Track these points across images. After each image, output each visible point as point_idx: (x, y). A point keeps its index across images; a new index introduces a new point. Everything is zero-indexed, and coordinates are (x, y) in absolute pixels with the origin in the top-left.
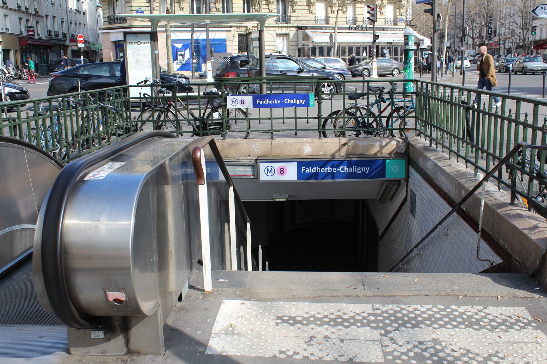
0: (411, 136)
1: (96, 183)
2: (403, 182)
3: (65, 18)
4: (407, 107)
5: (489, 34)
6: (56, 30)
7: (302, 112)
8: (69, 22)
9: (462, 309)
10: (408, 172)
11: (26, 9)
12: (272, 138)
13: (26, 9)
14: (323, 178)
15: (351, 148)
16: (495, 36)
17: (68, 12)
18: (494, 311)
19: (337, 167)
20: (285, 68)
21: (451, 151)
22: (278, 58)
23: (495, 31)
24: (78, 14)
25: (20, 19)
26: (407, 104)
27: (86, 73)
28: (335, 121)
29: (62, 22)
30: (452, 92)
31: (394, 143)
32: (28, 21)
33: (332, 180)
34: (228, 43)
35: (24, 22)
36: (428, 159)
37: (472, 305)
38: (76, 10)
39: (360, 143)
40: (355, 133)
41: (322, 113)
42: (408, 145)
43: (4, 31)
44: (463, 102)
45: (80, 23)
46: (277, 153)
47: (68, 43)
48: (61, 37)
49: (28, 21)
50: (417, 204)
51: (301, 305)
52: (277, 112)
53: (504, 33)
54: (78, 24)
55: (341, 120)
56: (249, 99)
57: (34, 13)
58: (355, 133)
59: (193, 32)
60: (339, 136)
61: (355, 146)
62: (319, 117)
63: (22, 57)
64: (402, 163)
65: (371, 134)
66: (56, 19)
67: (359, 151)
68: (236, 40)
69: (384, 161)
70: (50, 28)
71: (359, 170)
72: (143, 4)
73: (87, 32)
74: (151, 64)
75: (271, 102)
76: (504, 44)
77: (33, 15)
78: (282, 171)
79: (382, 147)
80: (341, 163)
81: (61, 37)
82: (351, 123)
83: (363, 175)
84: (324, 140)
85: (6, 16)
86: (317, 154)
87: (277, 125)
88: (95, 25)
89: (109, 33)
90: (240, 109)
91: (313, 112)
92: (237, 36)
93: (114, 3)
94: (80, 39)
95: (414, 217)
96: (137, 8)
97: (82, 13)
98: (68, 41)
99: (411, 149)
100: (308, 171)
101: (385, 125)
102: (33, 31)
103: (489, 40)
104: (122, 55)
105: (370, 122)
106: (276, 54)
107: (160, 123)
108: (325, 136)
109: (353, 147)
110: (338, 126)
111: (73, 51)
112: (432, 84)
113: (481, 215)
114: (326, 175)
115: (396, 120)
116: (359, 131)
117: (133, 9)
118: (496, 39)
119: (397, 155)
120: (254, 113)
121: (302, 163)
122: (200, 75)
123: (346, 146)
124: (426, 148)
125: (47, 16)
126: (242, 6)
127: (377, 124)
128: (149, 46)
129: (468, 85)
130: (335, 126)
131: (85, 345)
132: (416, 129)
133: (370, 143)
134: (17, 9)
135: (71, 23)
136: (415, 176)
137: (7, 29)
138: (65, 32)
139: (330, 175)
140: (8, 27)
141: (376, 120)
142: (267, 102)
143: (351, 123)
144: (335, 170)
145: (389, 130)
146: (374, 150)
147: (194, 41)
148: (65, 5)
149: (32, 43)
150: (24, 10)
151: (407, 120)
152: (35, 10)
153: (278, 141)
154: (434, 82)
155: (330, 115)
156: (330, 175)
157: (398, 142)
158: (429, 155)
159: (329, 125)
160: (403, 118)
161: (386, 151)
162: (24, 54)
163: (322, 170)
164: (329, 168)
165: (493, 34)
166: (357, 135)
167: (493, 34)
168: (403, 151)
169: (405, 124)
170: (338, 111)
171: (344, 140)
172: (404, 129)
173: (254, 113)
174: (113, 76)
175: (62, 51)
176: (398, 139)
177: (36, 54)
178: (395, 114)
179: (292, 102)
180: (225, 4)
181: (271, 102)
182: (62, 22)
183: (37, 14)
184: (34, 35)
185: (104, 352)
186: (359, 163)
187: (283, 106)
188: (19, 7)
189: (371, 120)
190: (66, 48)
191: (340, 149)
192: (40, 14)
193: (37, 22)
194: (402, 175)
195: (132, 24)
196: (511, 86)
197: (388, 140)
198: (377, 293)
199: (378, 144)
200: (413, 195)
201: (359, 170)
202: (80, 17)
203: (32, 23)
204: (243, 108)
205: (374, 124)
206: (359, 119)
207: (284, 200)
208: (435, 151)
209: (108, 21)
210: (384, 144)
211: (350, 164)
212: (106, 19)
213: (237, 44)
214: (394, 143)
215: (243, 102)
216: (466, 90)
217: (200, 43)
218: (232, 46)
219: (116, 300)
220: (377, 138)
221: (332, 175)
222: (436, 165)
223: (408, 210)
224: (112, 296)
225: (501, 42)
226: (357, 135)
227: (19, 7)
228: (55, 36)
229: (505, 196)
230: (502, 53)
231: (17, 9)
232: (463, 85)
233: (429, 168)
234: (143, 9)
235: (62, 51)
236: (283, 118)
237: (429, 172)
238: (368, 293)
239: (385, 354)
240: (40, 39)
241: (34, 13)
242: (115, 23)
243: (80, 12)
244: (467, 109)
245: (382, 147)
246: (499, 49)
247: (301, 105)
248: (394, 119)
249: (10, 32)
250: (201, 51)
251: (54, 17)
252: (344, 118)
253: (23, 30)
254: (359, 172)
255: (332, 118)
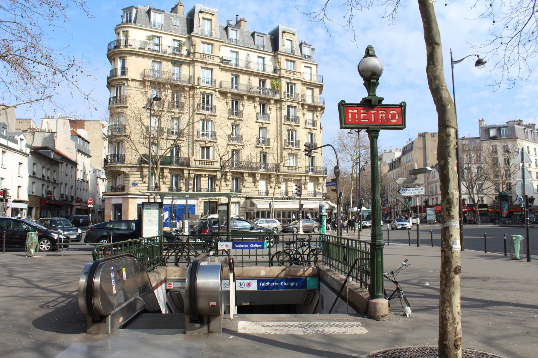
0: (320, 265)
1: (204, 267)
2: (317, 291)
3: (74, 185)
4: (318, 249)
5: (383, 202)
6: (67, 194)
7: (260, 251)
8: (76, 188)
9: (335, 323)
10: (319, 285)
11: (48, 178)
12: (243, 267)
13: (48, 178)
14: (272, 289)
15: (287, 272)
16: (388, 203)
17: (76, 181)
18: (347, 323)
19: (280, 283)
20: (242, 226)
21: (339, 270)
22: (237, 220)
23: (387, 200)
24: (83, 183)
25: (43, 185)
26: (318, 247)
27: (111, 226)
28: (278, 257)
29: (72, 188)
30: (352, 243)
31: (311, 269)
32: (48, 186)
33: (277, 290)
34: (196, 207)
35: (45, 187)
36: (328, 275)
37: (339, 321)
38: (82, 180)
39: (292, 269)
40: (289, 264)
41: (271, 252)
42: (319, 270)
43: (31, 193)
44: (342, 244)
45: (84, 189)
46: (245, 274)
47: (74, 203)
48: (70, 199)
49: (48, 186)
50: (324, 302)
51: (270, 322)
52: (246, 252)
53: (394, 201)
54: (82, 189)
55: (281, 256)
56: (230, 244)
57: (53, 181)
58: (289, 264)
59: (173, 199)
60: (281, 266)
61: (290, 271)
62: (269, 254)
63: (41, 213)
64: (316, 279)
65: (299, 265)
66: (68, 186)
67: (292, 273)
68: (202, 205)
69: (306, 279)
70: (62, 192)
71: (292, 284)
72: (137, 179)
73: (88, 195)
74: (158, 222)
75: (243, 246)
76: (394, 209)
77: (52, 182)
78: (249, 285)
79: (304, 271)
80: (282, 280)
81: (70, 199)
82: (287, 258)
83: (294, 287)
84: (272, 268)
85: (33, 183)
86: (268, 275)
87: (246, 258)
88: (94, 190)
89: (111, 198)
90: (224, 250)
91: (266, 251)
92: (203, 203)
93: (116, 177)
94: (90, 202)
95: (323, 309)
96: (133, 181)
97: (86, 182)
98: (74, 201)
99: (320, 271)
100: (263, 285)
101: (306, 259)
102: (51, 194)
103: (384, 206)
104: (119, 214)
105: (298, 257)
106: (236, 217)
107: (178, 257)
108: (272, 265)
109: (288, 271)
110: (280, 260)
111: (77, 209)
112: (338, 238)
113: (348, 293)
114: (274, 287)
115: (312, 257)
116: (292, 263)
117: (130, 182)
118: (388, 205)
119: (312, 275)
120: (233, 252)
121: (260, 280)
122: (176, 230)
123: (285, 271)
124: (328, 270)
125: (62, 183)
126: (207, 182)
127: (302, 259)
128: (158, 211)
129: (362, 238)
130: (278, 260)
131: (192, 330)
132: (323, 261)
133: (297, 269)
134: (42, 178)
135: (77, 189)
136: (323, 287)
137: (33, 193)
138: (73, 195)
139: (276, 287)
140: (34, 191)
141: (301, 256)
142: (240, 246)
143: (287, 258)
144: (279, 284)
145: (308, 262)
146: (300, 273)
147: (173, 206)
148: (75, 176)
149: (49, 202)
150: (46, 178)
151: (318, 256)
152: (54, 179)
153: (246, 268)
154: (339, 236)
155: (275, 254)
156: (276, 287)
157: (313, 268)
158: (330, 274)
159: (275, 259)
160: (316, 255)
161: (307, 273)
162: (42, 211)
163: (271, 284)
164: (275, 283)
165: (386, 202)
166: (291, 265)
167: (386, 202)
168: (316, 273)
169: (317, 259)
170: (280, 251)
171: (283, 268)
172: (317, 261)
173: (233, 252)
174: (129, 229)
175: (69, 209)
176: (313, 267)
177: (50, 211)
178: (312, 253)
179: (254, 246)
180: (196, 180)
181: (243, 246)
182: (72, 188)
183: (55, 182)
184: (51, 197)
185: (199, 332)
186: (292, 280)
187: (249, 248)
188: (43, 176)
189: (298, 256)
190: (72, 206)
191: (281, 273)
192: (57, 182)
193: (54, 188)
194: (316, 287)
195: (129, 192)
196: (390, 238)
197: (308, 267)
198: (301, 319)
199: (302, 270)
200: (322, 297)
201: (292, 284)
202: (84, 184)
203: (51, 188)
204: (226, 249)
205: (300, 259)
206: (292, 256)
207: (248, 304)
208: (332, 271)
209: (111, 190)
210: (305, 269)
211: (287, 281)
212: (110, 188)
213: (203, 208)
214: (311, 269)
215: (227, 246)
216: (343, 238)
217: (176, 207)
218: (199, 210)
219: (213, 306)
220: (302, 266)
221: (277, 287)
222: (332, 277)
223: (320, 306)
224: (212, 303)
225: (392, 207)
226: (291, 265)
227: (43, 176)
228: (66, 198)
229: (358, 285)
230: (393, 215)
231: (41, 178)
232: (359, 239)
233: (328, 280)
234: (137, 182)
235: (69, 209)
236: (249, 255)
237: (329, 282)
238: (297, 319)
239: (304, 333)
240: (55, 200)
241: (53, 181)
242: (116, 191)
243: (84, 181)
244: (344, 248)
245: (304, 271)
246: (391, 213)
247: (259, 248)
248: (311, 256)
249: (35, 194)
250: (177, 213)
251: (66, 184)
252: (283, 255)
253: (44, 193)
254: (292, 285)
255: (276, 255)
